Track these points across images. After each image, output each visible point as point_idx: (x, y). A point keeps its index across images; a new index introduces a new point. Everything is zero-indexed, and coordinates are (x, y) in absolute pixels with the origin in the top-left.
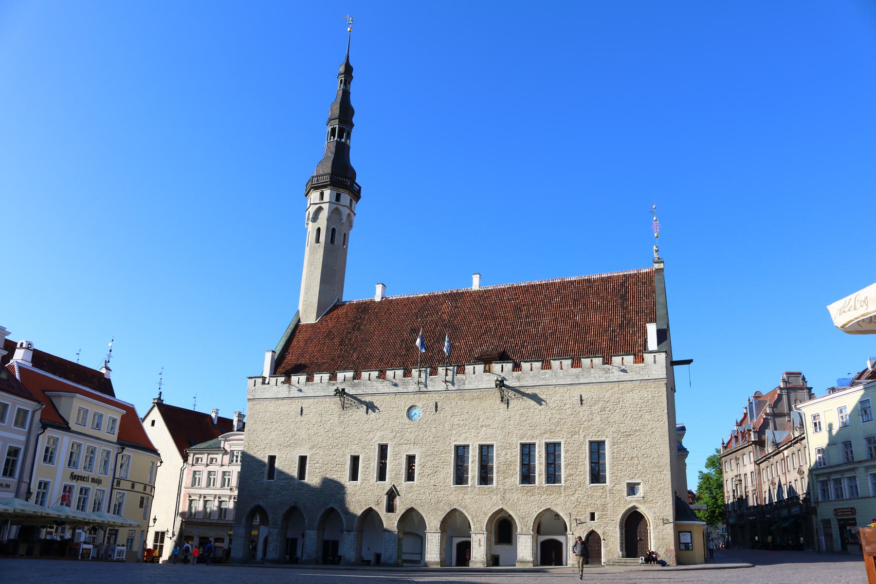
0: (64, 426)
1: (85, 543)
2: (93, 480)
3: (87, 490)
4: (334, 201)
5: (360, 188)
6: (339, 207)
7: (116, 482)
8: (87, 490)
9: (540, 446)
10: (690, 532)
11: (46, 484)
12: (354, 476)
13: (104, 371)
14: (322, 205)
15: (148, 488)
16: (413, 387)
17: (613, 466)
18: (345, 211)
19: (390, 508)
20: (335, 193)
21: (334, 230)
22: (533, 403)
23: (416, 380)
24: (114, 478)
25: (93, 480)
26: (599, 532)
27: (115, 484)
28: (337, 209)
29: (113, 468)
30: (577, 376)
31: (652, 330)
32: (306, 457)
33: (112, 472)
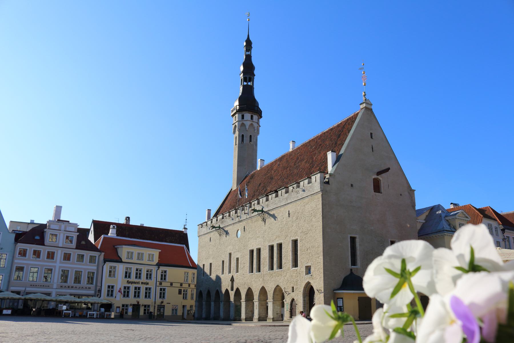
0: (120, 261)
1: (65, 310)
2: (142, 283)
3: (139, 288)
4: (240, 119)
6: (244, 122)
8: (139, 288)
10: (342, 298)
11: (113, 287)
12: (223, 273)
13: (183, 230)
16: (237, 220)
18: (248, 124)
19: (232, 289)
20: (241, 115)
21: (243, 136)
22: (273, 219)
25: (142, 283)
26: (295, 299)
27: (158, 283)
30: (287, 199)
31: (330, 156)
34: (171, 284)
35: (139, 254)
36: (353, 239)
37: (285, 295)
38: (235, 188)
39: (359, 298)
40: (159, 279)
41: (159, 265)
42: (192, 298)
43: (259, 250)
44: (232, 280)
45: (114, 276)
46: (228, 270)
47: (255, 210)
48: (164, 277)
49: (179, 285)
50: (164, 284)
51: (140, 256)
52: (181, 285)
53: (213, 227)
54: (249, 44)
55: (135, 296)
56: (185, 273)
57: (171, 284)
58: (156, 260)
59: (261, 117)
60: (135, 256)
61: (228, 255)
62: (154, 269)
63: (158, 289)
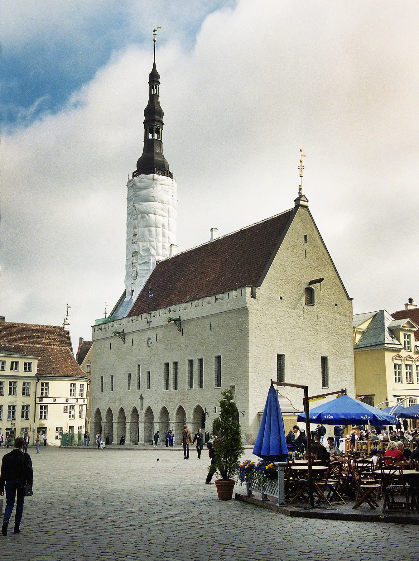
16: (147, 326)
27: (38, 400)
34: (55, 399)
35: (12, 363)
36: (280, 357)
37: (206, 415)
40: (39, 394)
41: (38, 377)
42: (80, 417)
43: (176, 364)
44: (141, 398)
46: (136, 385)
47: (172, 320)
48: (44, 392)
49: (64, 401)
50: (45, 400)
51: (14, 367)
52: (67, 400)
53: (117, 333)
56: (71, 384)
57: (55, 399)
58: (35, 369)
61: (137, 368)
62: (33, 383)
63: (38, 407)
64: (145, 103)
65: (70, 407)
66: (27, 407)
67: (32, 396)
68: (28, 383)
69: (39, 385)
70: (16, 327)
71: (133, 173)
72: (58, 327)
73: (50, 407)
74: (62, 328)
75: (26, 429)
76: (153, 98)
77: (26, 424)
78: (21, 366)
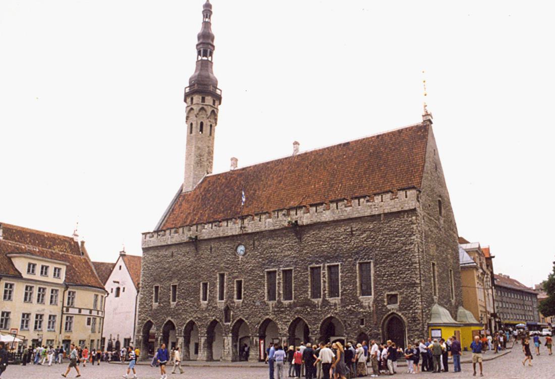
0: (18, 276)
5: (221, 91)
6: (205, 107)
7: (65, 310)
9: (324, 268)
11: (8, 313)
14: (193, 107)
15: (100, 313)
17: (376, 282)
21: (202, 124)
23: (240, 226)
24: (63, 307)
27: (65, 309)
28: (202, 109)
29: (62, 300)
32: (176, 286)
33: (61, 303)
34: (80, 310)
35: (42, 267)
38: (189, 189)
39: (455, 331)
40: (66, 304)
42: (99, 332)
45: (10, 298)
49: (87, 312)
50: (71, 311)
52: (91, 313)
54: (207, 11)
55: (36, 328)
57: (80, 310)
59: (220, 104)
60: (38, 269)
62: (61, 291)
64: (199, 29)
65: (93, 318)
66: (54, 316)
67: (60, 305)
68: (57, 291)
69: (67, 293)
70: (29, 233)
71: (186, 88)
72: (68, 238)
73: (75, 319)
74: (72, 239)
75: (52, 341)
76: (207, 25)
77: (51, 336)
78: (51, 271)
